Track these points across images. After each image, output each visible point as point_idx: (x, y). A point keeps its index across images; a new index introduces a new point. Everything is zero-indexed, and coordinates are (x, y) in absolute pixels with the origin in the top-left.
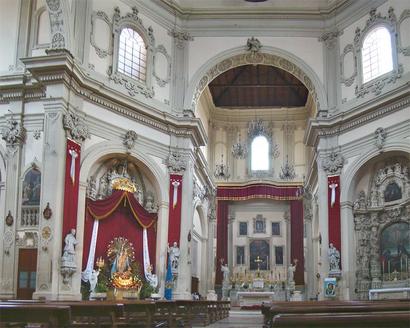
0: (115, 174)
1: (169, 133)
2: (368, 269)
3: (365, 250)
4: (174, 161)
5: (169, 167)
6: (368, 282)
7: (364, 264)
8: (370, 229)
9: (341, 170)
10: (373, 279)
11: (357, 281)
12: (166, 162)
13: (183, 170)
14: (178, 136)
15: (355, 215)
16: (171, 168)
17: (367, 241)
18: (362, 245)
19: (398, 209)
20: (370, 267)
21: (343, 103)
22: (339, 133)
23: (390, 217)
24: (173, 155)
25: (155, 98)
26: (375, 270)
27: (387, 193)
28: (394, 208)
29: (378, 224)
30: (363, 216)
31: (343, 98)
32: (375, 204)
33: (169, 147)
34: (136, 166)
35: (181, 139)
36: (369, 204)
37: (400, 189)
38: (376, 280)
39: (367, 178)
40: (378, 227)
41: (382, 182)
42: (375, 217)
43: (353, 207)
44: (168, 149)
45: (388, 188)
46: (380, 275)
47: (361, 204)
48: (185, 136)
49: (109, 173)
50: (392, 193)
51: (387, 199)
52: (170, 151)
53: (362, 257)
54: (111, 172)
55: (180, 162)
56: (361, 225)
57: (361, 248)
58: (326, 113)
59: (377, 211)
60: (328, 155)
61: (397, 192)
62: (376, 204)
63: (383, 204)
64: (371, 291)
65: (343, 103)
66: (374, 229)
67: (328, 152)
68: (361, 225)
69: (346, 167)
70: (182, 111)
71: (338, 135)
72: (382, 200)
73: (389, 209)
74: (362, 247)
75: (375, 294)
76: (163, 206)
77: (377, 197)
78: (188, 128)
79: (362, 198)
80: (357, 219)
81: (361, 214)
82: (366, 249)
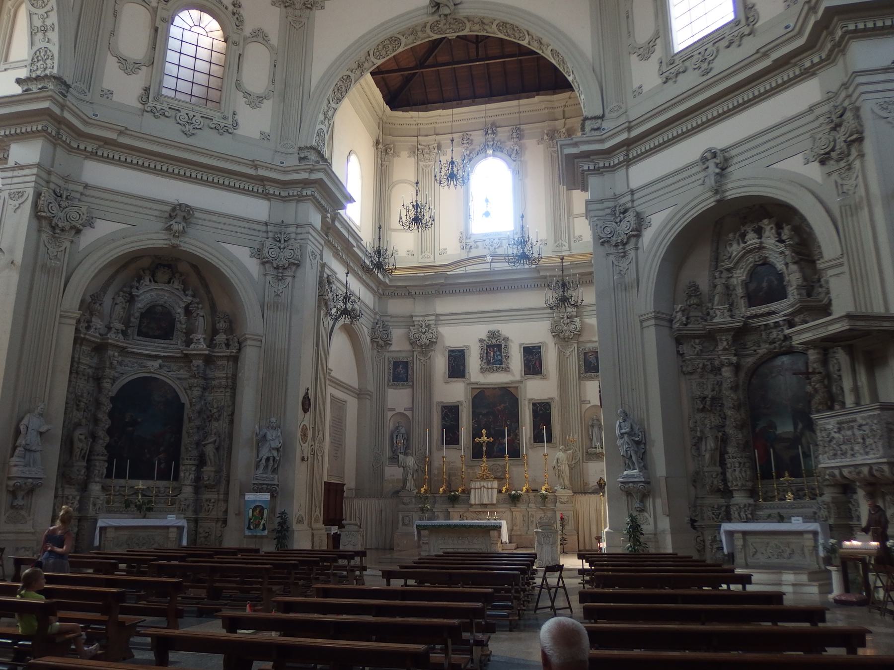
0: (148, 283)
1: (266, 196)
2: (719, 469)
3: (707, 422)
4: (275, 252)
5: (263, 263)
6: (722, 501)
7: (707, 456)
8: (717, 370)
9: (636, 244)
10: (735, 494)
11: (697, 498)
12: (258, 253)
13: (294, 268)
14: (284, 199)
15: (679, 341)
16: (267, 265)
17: (713, 399)
18: (703, 410)
19: (781, 323)
20: (722, 463)
21: (635, 97)
22: (629, 162)
23: (765, 342)
24: (274, 239)
25: (240, 132)
26: (737, 474)
27: (752, 286)
28: (771, 320)
29: (734, 359)
30: (697, 341)
31: (636, 85)
32: (723, 314)
33: (266, 224)
34: (195, 267)
35: (293, 205)
36: (711, 312)
37: (780, 276)
38: (740, 499)
39: (703, 256)
40: (737, 368)
41: (737, 262)
42: (725, 343)
43: (671, 321)
44: (264, 228)
45: (752, 274)
46: (750, 484)
47: (692, 314)
48: (300, 199)
49: (135, 283)
50: (765, 285)
51: (753, 299)
52: (267, 232)
53: (700, 439)
54: (138, 281)
55: (287, 253)
56: (696, 362)
57: (699, 416)
58: (600, 121)
59: (728, 330)
60: (609, 211)
61: (776, 282)
62: (727, 314)
63: (744, 310)
64: (726, 526)
65: (635, 97)
66: (727, 372)
67: (606, 205)
68: (696, 362)
69: (648, 235)
70: (296, 150)
71: (628, 166)
72: (742, 303)
73: (761, 322)
74: (701, 415)
75: (736, 535)
76: (249, 342)
77: (729, 295)
78: (306, 183)
79: (694, 301)
80: (685, 348)
81: (695, 337)
82: (713, 419)
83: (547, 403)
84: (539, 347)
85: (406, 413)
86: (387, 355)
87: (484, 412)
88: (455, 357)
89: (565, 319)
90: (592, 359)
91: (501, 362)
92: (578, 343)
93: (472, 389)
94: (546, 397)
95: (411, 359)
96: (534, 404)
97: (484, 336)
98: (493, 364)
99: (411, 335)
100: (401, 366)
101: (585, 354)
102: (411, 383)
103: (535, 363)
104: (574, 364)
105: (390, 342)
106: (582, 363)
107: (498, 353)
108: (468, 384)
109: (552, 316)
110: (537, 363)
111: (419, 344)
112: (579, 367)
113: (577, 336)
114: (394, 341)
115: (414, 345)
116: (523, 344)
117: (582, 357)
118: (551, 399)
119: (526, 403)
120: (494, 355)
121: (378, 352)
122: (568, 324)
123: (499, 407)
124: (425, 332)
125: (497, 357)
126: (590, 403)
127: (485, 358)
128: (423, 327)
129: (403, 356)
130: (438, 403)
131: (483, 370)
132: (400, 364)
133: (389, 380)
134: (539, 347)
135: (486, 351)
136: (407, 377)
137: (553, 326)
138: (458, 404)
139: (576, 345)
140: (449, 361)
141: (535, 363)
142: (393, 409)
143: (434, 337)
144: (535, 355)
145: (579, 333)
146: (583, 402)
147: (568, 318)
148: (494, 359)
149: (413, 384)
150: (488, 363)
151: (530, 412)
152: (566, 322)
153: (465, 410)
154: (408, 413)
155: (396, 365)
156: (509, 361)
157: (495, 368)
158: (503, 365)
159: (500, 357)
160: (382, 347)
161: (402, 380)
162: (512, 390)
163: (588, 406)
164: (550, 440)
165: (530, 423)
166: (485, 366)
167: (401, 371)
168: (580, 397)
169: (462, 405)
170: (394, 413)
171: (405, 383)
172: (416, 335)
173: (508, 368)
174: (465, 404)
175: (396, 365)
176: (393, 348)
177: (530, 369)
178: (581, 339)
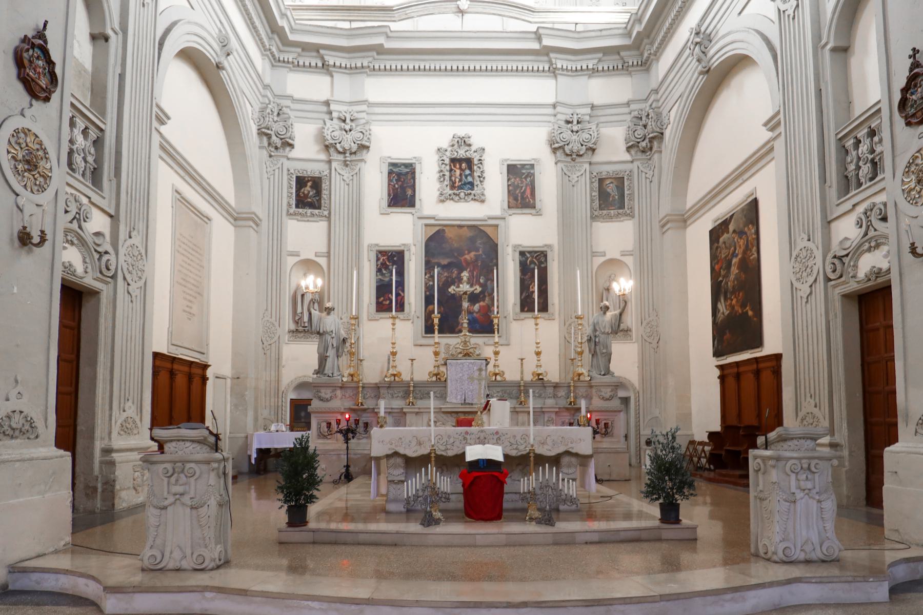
83: (542, 252)
84: (532, 166)
85: (317, 259)
86: (287, 164)
87: (445, 262)
88: (399, 175)
89: (575, 122)
90: (611, 188)
91: (472, 185)
92: (590, 163)
93: (426, 225)
94: (541, 245)
95: (325, 173)
96: (522, 254)
97: (445, 144)
98: (460, 188)
99: (328, 134)
100: (309, 184)
101: (601, 181)
102: (326, 213)
103: (525, 190)
104: (584, 194)
105: (290, 141)
106: (596, 194)
107: (468, 172)
108: (419, 218)
109: (552, 119)
110: (528, 192)
111: (341, 150)
112: (592, 201)
113: (590, 152)
114: (296, 143)
115: (332, 150)
116: (506, 160)
117: (596, 185)
118: (549, 246)
119: (510, 250)
120: (461, 175)
121: (271, 156)
122: (577, 132)
123: (467, 257)
124: (350, 130)
125: (466, 178)
126: (605, 255)
127: (447, 178)
128: (348, 121)
129: (313, 169)
130: (370, 246)
131: (443, 198)
132: (308, 181)
133: (289, 205)
134: (532, 166)
135: (448, 168)
136: (319, 201)
137: (556, 133)
138: (402, 248)
139: (587, 166)
140: (390, 180)
141: (525, 190)
142: (296, 254)
143: (365, 138)
144: (526, 178)
145: (595, 147)
146: (594, 254)
147: (578, 122)
148: (460, 180)
149: (330, 214)
150: (453, 187)
151: (515, 264)
152: (575, 128)
153: (413, 258)
154: (323, 261)
155: (301, 182)
156: (484, 186)
157: (462, 195)
158: (476, 191)
159: (470, 179)
160: (276, 148)
161: (312, 206)
162: (489, 231)
163: (602, 259)
164: (544, 308)
165: (515, 283)
166: (448, 191)
167: (309, 192)
168: (591, 246)
169: (409, 250)
170: (297, 259)
171: (316, 211)
172: (335, 134)
173: (483, 195)
174: (413, 249)
175: (301, 182)
176: (294, 154)
177: (516, 199)
178: (597, 158)
